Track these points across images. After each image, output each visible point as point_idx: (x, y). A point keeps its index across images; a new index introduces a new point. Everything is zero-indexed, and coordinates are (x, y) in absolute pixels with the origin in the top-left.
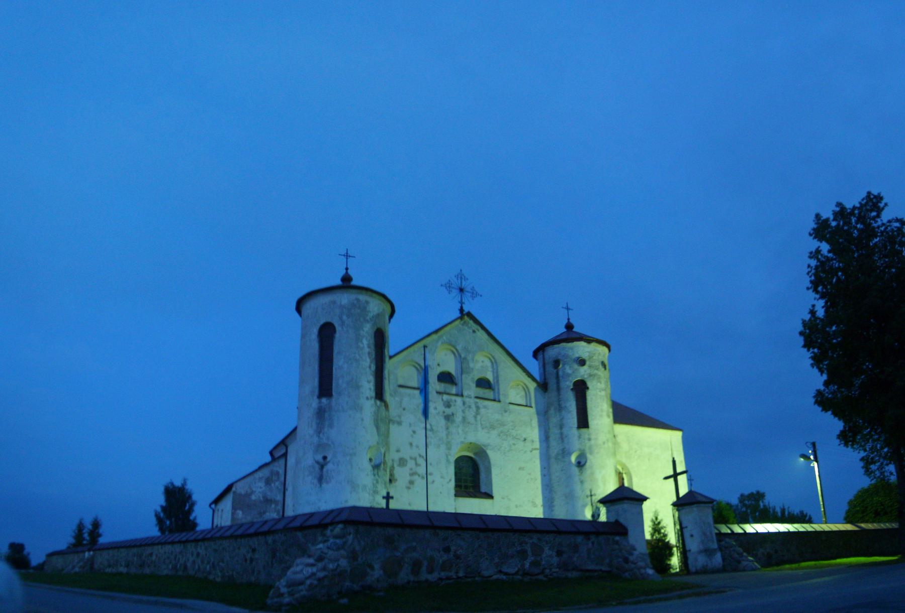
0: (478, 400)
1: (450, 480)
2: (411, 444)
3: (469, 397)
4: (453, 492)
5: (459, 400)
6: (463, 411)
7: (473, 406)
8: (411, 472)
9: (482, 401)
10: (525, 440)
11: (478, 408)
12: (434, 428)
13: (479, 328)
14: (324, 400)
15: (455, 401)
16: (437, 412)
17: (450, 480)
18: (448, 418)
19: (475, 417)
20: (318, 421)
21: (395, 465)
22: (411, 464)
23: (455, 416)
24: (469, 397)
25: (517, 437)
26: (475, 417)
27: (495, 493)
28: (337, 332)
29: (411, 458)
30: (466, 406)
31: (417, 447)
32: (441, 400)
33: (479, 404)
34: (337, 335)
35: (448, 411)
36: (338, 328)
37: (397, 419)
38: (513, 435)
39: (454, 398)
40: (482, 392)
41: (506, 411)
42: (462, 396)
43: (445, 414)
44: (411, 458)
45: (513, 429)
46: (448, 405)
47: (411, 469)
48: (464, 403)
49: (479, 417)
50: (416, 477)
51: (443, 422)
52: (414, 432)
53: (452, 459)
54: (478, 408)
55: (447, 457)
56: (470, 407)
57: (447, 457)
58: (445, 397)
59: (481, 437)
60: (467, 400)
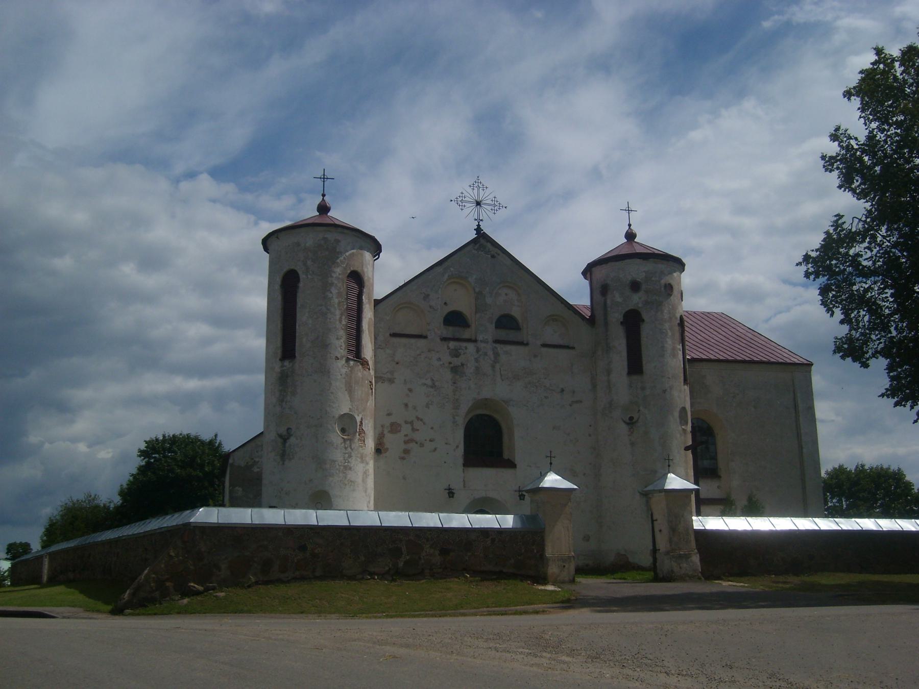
0: (497, 345)
1: (457, 447)
2: (406, 405)
3: (485, 341)
4: (461, 461)
5: (471, 347)
6: (477, 360)
7: (490, 353)
8: (407, 438)
9: (502, 346)
10: (562, 390)
11: (496, 355)
12: (437, 384)
13: (499, 252)
14: (287, 363)
15: (466, 348)
16: (441, 363)
17: (457, 447)
18: (455, 370)
19: (493, 367)
20: (281, 388)
21: (386, 432)
22: (406, 429)
23: (465, 366)
24: (485, 341)
25: (551, 388)
26: (493, 367)
27: (517, 460)
28: (301, 280)
29: (406, 422)
30: (480, 353)
31: (415, 408)
32: (446, 347)
33: (499, 349)
34: (301, 285)
35: (457, 361)
36: (302, 276)
37: (389, 376)
38: (545, 386)
39: (464, 344)
40: (503, 334)
41: (535, 356)
42: (475, 341)
43: (452, 365)
44: (406, 422)
45: (545, 379)
46: (456, 354)
47: (406, 435)
48: (478, 350)
49: (498, 366)
50: (412, 445)
51: (448, 375)
52: (410, 390)
53: (462, 422)
54: (496, 355)
55: (454, 418)
56: (486, 354)
57: (454, 418)
58: (452, 344)
59: (498, 390)
60: (482, 345)
